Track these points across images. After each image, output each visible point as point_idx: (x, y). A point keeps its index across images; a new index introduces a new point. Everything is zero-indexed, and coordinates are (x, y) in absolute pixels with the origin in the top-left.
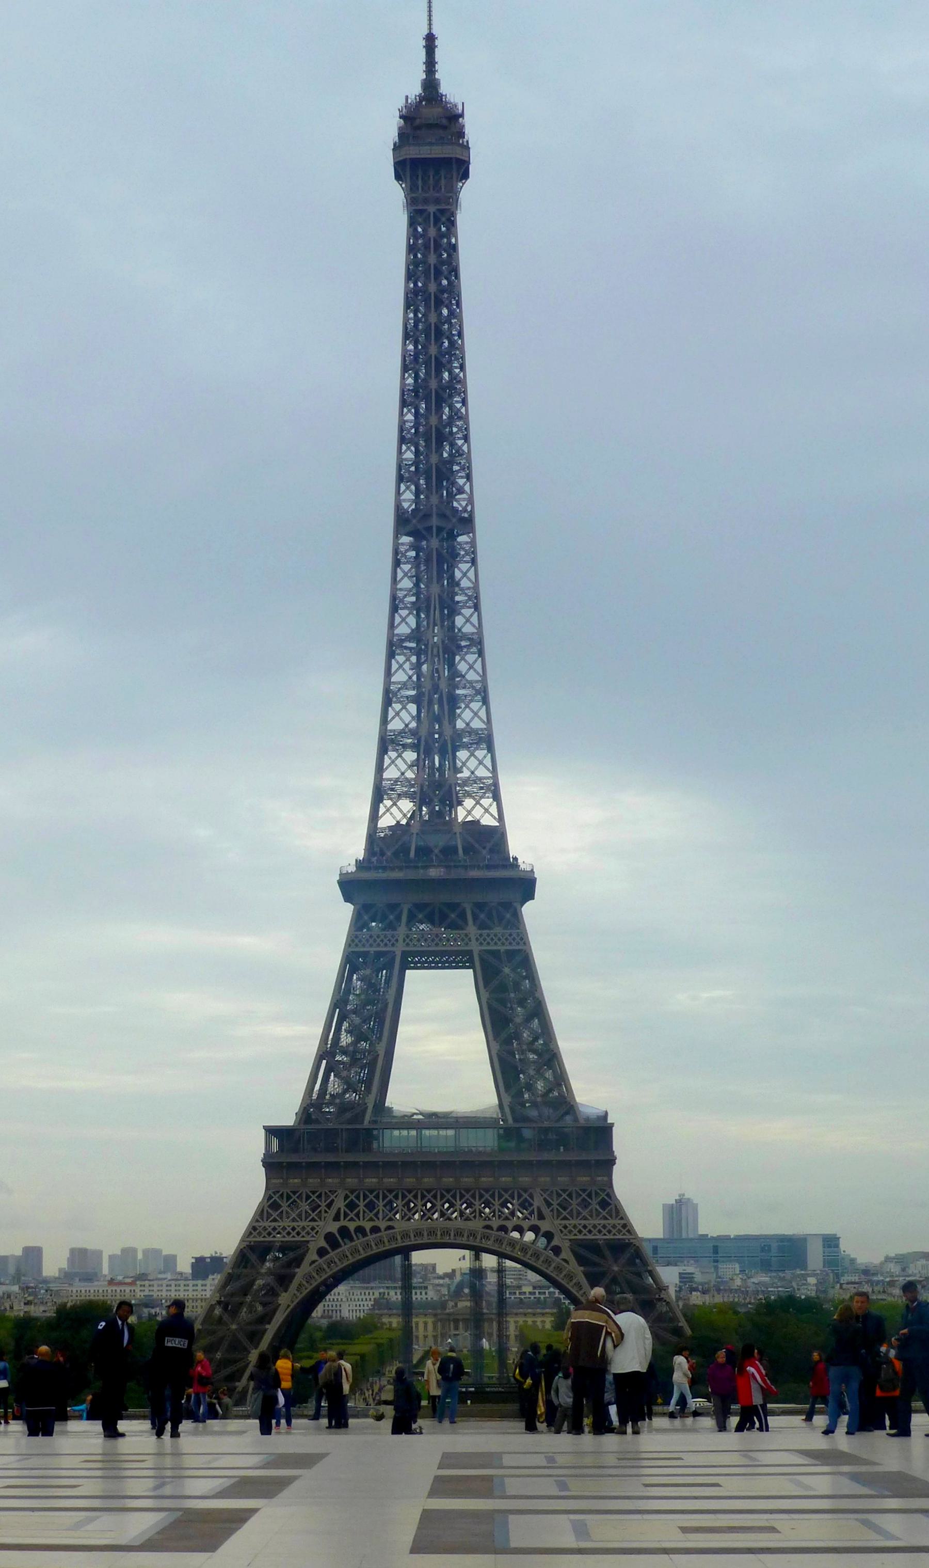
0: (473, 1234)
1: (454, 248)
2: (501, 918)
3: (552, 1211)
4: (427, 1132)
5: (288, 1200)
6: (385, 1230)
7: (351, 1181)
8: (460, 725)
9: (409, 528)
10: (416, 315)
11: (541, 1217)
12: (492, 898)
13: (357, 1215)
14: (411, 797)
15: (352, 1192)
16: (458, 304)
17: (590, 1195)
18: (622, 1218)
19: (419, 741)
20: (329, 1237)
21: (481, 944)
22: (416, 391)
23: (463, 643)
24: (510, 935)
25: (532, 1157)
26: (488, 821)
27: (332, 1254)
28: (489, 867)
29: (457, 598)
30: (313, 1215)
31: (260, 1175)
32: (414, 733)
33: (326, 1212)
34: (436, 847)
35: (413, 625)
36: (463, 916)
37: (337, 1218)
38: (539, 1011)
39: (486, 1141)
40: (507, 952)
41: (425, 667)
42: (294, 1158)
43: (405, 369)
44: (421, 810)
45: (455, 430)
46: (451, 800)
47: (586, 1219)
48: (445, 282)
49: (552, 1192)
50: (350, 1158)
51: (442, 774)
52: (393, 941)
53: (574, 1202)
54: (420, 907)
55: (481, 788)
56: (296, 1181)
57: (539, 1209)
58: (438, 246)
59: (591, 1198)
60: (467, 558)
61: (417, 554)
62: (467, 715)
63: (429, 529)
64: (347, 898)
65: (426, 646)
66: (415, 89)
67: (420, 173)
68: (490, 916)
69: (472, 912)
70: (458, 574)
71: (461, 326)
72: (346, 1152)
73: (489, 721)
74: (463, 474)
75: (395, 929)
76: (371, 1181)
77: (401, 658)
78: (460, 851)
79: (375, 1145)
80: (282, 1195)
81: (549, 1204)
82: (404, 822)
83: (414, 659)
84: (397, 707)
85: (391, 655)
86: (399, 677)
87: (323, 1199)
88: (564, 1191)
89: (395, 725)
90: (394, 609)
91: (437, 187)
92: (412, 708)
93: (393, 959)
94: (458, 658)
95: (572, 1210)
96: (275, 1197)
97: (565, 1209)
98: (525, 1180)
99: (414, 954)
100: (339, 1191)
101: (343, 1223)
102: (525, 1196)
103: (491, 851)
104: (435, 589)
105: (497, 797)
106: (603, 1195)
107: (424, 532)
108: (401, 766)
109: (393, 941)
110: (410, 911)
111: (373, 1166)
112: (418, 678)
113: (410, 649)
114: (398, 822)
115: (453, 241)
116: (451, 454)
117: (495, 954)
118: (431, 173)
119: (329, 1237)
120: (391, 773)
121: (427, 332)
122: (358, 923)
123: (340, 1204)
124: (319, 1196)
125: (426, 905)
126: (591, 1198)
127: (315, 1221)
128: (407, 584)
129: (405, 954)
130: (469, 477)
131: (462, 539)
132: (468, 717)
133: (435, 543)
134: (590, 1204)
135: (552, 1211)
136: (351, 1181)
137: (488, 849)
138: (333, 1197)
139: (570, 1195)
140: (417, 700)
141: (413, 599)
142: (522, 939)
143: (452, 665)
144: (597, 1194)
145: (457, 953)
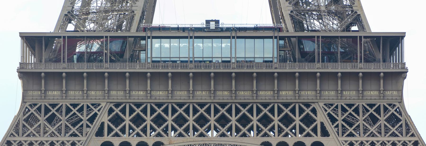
3: (337, 126)
4: (199, 44)
5: (46, 114)
11: (325, 133)
15: (117, 105)
17: (378, 111)
18: (413, 135)
25: (317, 68)
30: (74, 130)
31: (17, 85)
33: (88, 126)
37: (100, 133)
42: (53, 68)
47: (373, 135)
49: (337, 107)
50: (117, 68)
53: (361, 119)
56: (55, 93)
57: (322, 124)
59: (380, 114)
72: (111, 61)
79: (143, 55)
80: (39, 109)
81: (333, 120)
88: (350, 106)
95: (358, 126)
96: (32, 111)
97: (351, 125)
98: (308, 94)
100: (103, 104)
102: (308, 111)
106: (393, 111)
111: (139, 77)
123: (104, 118)
124: (81, 110)
126: (380, 114)
127: (75, 135)
134: (378, 119)
135: (337, 126)
136: (117, 95)
138: (96, 110)
139: (356, 111)
144: (386, 109)
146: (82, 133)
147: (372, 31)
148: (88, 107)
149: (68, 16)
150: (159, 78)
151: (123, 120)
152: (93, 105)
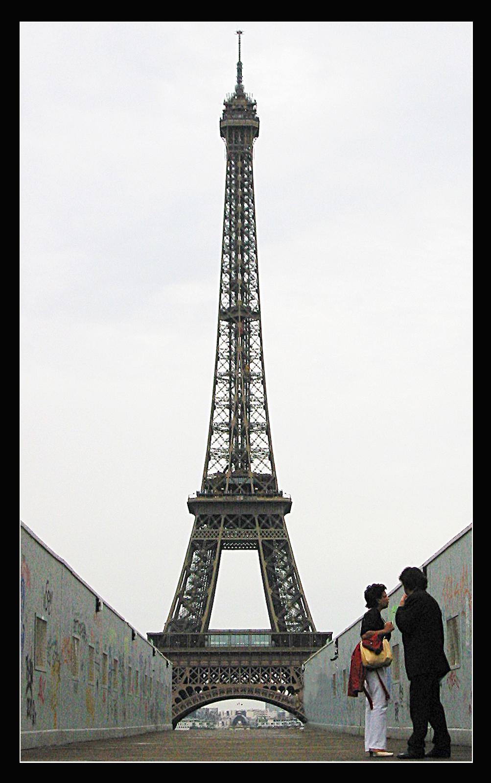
0: (257, 691)
1: (251, 172)
2: (273, 523)
6: (212, 688)
7: (194, 663)
8: (252, 420)
9: (226, 317)
10: (230, 207)
11: (294, 682)
12: (269, 512)
13: (196, 681)
14: (227, 458)
15: (194, 668)
16: (253, 202)
19: (230, 428)
20: (181, 693)
21: (263, 537)
22: (230, 246)
23: (254, 378)
24: (278, 532)
25: (290, 649)
26: (267, 471)
27: (183, 701)
28: (268, 496)
29: (251, 354)
32: (228, 424)
33: (180, 679)
34: (240, 484)
35: (228, 368)
36: (253, 522)
37: (186, 682)
38: (293, 571)
39: (266, 642)
40: (277, 540)
41: (233, 390)
43: (224, 235)
44: (231, 465)
45: (250, 267)
46: (247, 461)
48: (246, 190)
51: (243, 446)
52: (216, 534)
54: (231, 516)
55: (263, 454)
57: (293, 678)
58: (242, 172)
60: (257, 333)
61: (230, 331)
62: (256, 415)
63: (237, 318)
64: (191, 511)
65: (235, 379)
66: (233, 91)
67: (234, 133)
68: (267, 522)
69: (258, 520)
70: (251, 341)
71: (254, 213)
73: (267, 418)
74: (254, 289)
75: (217, 528)
76: (204, 663)
77: (221, 385)
78: (252, 485)
79: (206, 643)
82: (222, 471)
83: (228, 385)
84: (219, 410)
85: (216, 383)
86: (220, 395)
87: (178, 672)
89: (217, 420)
90: (218, 359)
91: (243, 142)
92: (227, 411)
93: (217, 544)
94: (251, 385)
99: (227, 541)
100: (187, 668)
101: (189, 685)
103: (269, 488)
104: (240, 350)
105: (271, 459)
107: (234, 320)
108: (221, 442)
109: (216, 534)
110: (225, 519)
112: (230, 396)
113: (226, 380)
114: (218, 471)
115: (250, 169)
116: (249, 280)
117: (270, 542)
118: (240, 134)
119: (181, 693)
120: (215, 445)
121: (236, 216)
122: (198, 524)
123: (188, 674)
125: (234, 516)
128: (224, 346)
129: (222, 542)
130: (258, 291)
131: (254, 323)
132: (256, 416)
133: (240, 325)
137: (266, 486)
138: (183, 671)
140: (229, 407)
141: (228, 354)
142: (284, 534)
143: (248, 389)
145: (249, 541)
146: (177, 682)
147: (318, 631)
148: (180, 669)
149: (169, 624)
150: (216, 654)
151: (197, 676)
152: (182, 668)
